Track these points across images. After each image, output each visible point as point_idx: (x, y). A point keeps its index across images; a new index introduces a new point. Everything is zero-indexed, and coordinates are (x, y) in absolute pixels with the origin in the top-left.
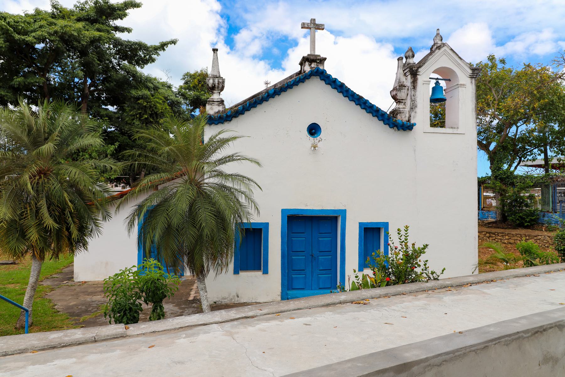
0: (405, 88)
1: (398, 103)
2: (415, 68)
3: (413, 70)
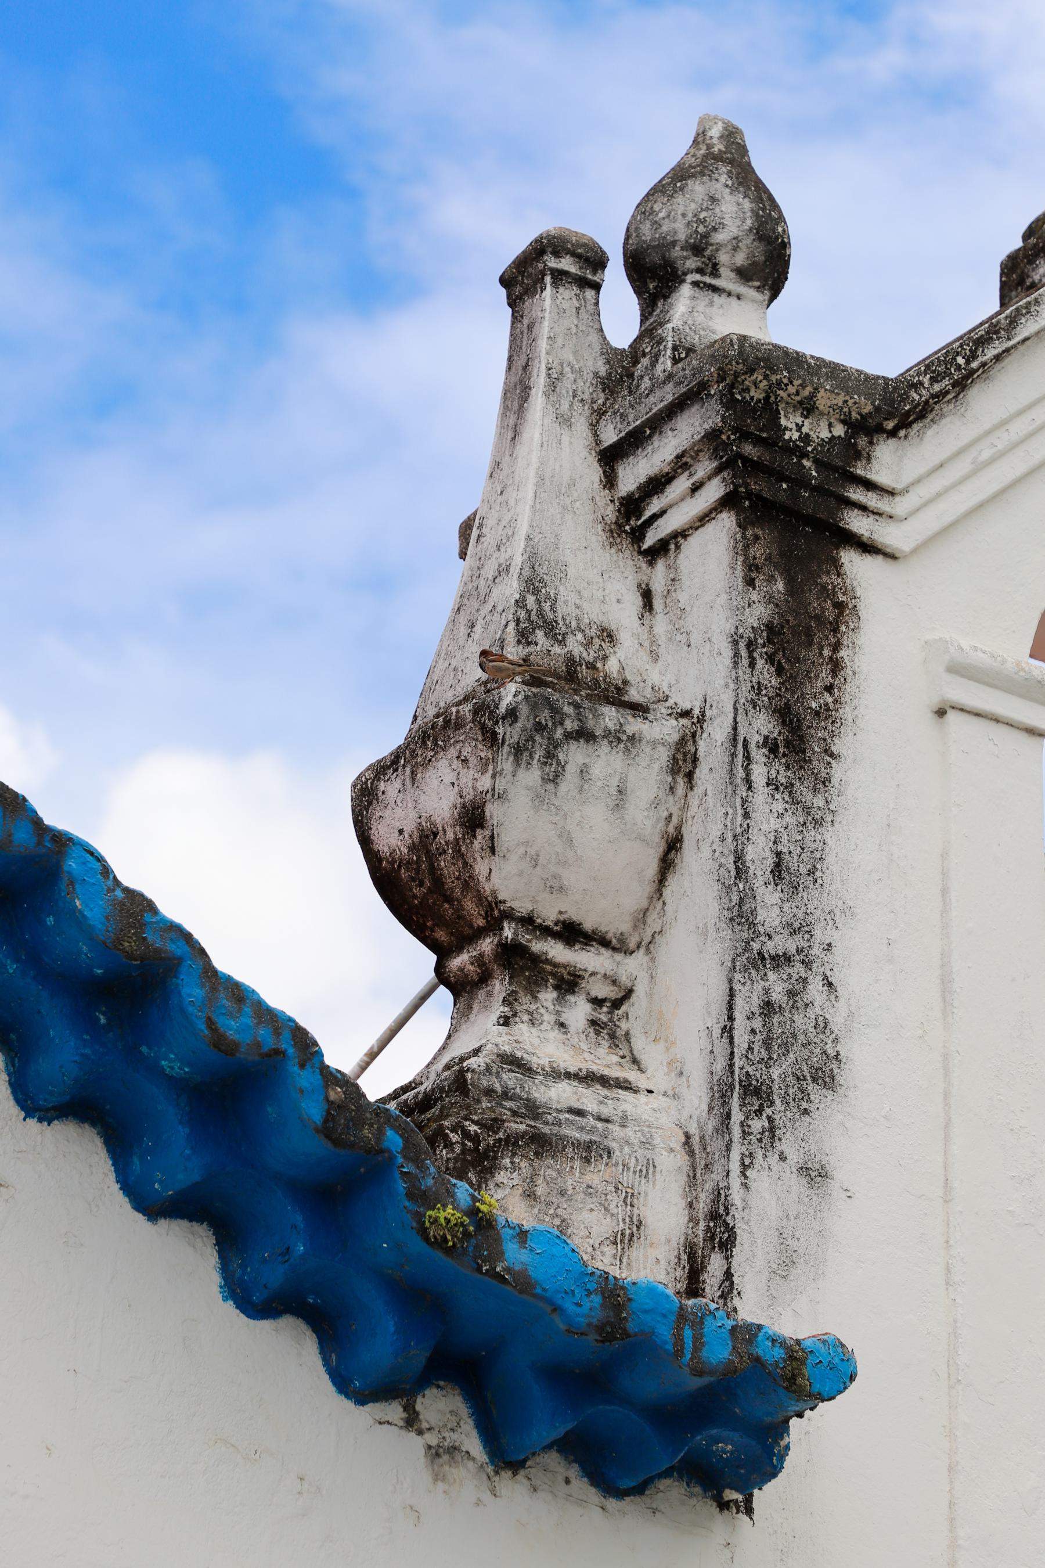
0: (634, 725)
1: (499, 987)
2: (808, 408)
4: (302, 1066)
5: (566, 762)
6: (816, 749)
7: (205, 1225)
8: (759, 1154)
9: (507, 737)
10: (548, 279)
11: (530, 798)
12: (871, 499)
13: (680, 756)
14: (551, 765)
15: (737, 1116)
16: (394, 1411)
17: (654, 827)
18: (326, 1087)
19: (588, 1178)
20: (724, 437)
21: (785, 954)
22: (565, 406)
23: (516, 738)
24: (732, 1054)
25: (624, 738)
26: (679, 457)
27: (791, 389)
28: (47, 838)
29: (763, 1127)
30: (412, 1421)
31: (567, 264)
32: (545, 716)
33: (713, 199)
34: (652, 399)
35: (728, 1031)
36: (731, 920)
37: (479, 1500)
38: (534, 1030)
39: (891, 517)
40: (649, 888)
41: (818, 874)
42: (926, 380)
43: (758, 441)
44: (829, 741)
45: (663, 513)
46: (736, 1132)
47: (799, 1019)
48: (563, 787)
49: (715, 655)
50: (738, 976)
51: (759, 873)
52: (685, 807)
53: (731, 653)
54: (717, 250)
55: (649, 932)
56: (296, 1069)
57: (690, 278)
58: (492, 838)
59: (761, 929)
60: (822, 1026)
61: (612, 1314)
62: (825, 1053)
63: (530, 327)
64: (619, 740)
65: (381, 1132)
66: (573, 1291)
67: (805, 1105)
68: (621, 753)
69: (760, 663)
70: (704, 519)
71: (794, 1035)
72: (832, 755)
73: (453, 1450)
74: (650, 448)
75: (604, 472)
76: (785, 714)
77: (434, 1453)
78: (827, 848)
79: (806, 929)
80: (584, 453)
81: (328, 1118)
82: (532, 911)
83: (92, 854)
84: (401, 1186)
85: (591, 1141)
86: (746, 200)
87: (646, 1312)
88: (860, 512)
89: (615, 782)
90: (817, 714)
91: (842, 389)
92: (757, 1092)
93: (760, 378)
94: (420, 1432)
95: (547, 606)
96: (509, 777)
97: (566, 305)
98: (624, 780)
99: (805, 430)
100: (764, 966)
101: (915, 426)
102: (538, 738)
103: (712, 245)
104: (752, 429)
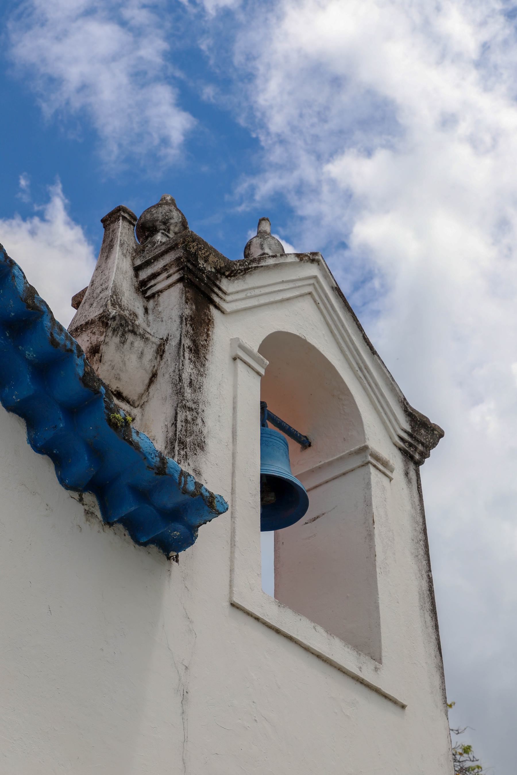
3: (196, 265)
4: (78, 357)
5: (128, 339)
6: (202, 355)
7: (24, 419)
8: (183, 461)
9: (112, 325)
10: (121, 218)
11: (115, 346)
12: (220, 293)
13: (159, 349)
14: (123, 338)
15: (177, 448)
16: (76, 495)
17: (150, 368)
18: (85, 366)
20: (182, 260)
21: (191, 408)
22: (125, 252)
23: (114, 326)
24: (176, 430)
25: (145, 337)
26: (165, 266)
27: (203, 252)
28: (8, 260)
29: (184, 454)
30: (81, 500)
31: (126, 215)
32: (123, 322)
33: (171, 211)
34: (156, 250)
35: (175, 424)
36: (177, 393)
37: (99, 531)
39: (224, 300)
40: (145, 387)
41: (201, 389)
42: (238, 264)
43: (192, 264)
44: (205, 354)
45: (155, 285)
46: (177, 453)
47: (195, 427)
48: (125, 346)
49: (173, 322)
50: (179, 409)
52: (159, 365)
53: (179, 320)
54: (171, 225)
55: (142, 402)
56: (76, 357)
57: (161, 231)
58: (101, 357)
60: (201, 432)
61: (162, 465)
62: (201, 440)
63: (113, 231)
64: (143, 338)
65: (99, 386)
66: (152, 454)
67: (195, 452)
68: (143, 342)
69: (188, 325)
70: (170, 286)
73: (92, 513)
74: (153, 266)
75: (135, 273)
76: (194, 341)
77: (87, 512)
79: (198, 403)
80: (130, 266)
81: (84, 376)
82: (109, 385)
83: (21, 270)
84: (104, 405)
86: (180, 214)
87: (172, 468)
88: (216, 296)
89: (141, 350)
90: (202, 346)
91: (217, 256)
92: (183, 443)
93: (195, 245)
94: (83, 505)
96: (110, 338)
97: (126, 226)
98: (143, 350)
99: (205, 266)
100: (186, 409)
101: (232, 278)
102: (120, 328)
103: (169, 223)
104: (191, 259)
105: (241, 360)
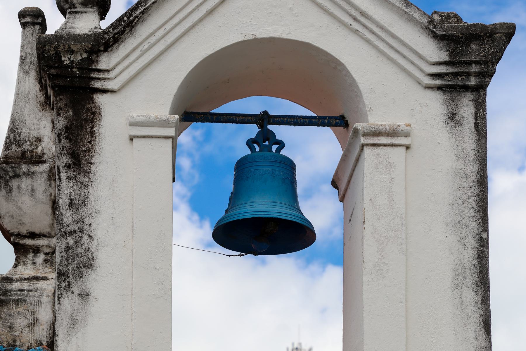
5: (12, 186)
13: (51, 175)
19: (18, 310)
25: (30, 173)
38: (24, 267)
48: (14, 193)
51: (64, 207)
59: (65, 225)
67: (81, 275)
71: (77, 255)
72: (91, 163)
78: (89, 194)
85: (18, 299)
95: (17, 136)
105: (138, 137)
